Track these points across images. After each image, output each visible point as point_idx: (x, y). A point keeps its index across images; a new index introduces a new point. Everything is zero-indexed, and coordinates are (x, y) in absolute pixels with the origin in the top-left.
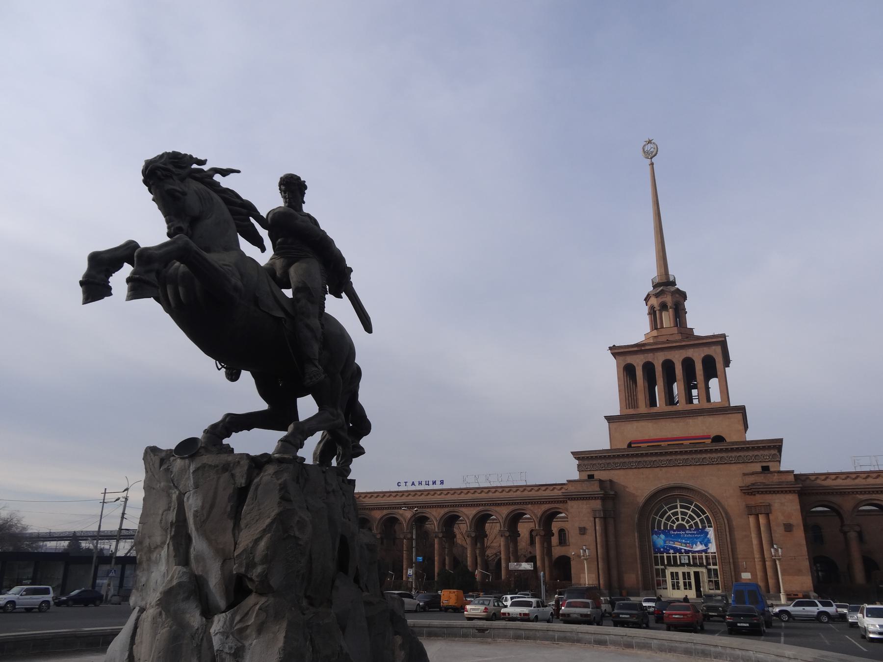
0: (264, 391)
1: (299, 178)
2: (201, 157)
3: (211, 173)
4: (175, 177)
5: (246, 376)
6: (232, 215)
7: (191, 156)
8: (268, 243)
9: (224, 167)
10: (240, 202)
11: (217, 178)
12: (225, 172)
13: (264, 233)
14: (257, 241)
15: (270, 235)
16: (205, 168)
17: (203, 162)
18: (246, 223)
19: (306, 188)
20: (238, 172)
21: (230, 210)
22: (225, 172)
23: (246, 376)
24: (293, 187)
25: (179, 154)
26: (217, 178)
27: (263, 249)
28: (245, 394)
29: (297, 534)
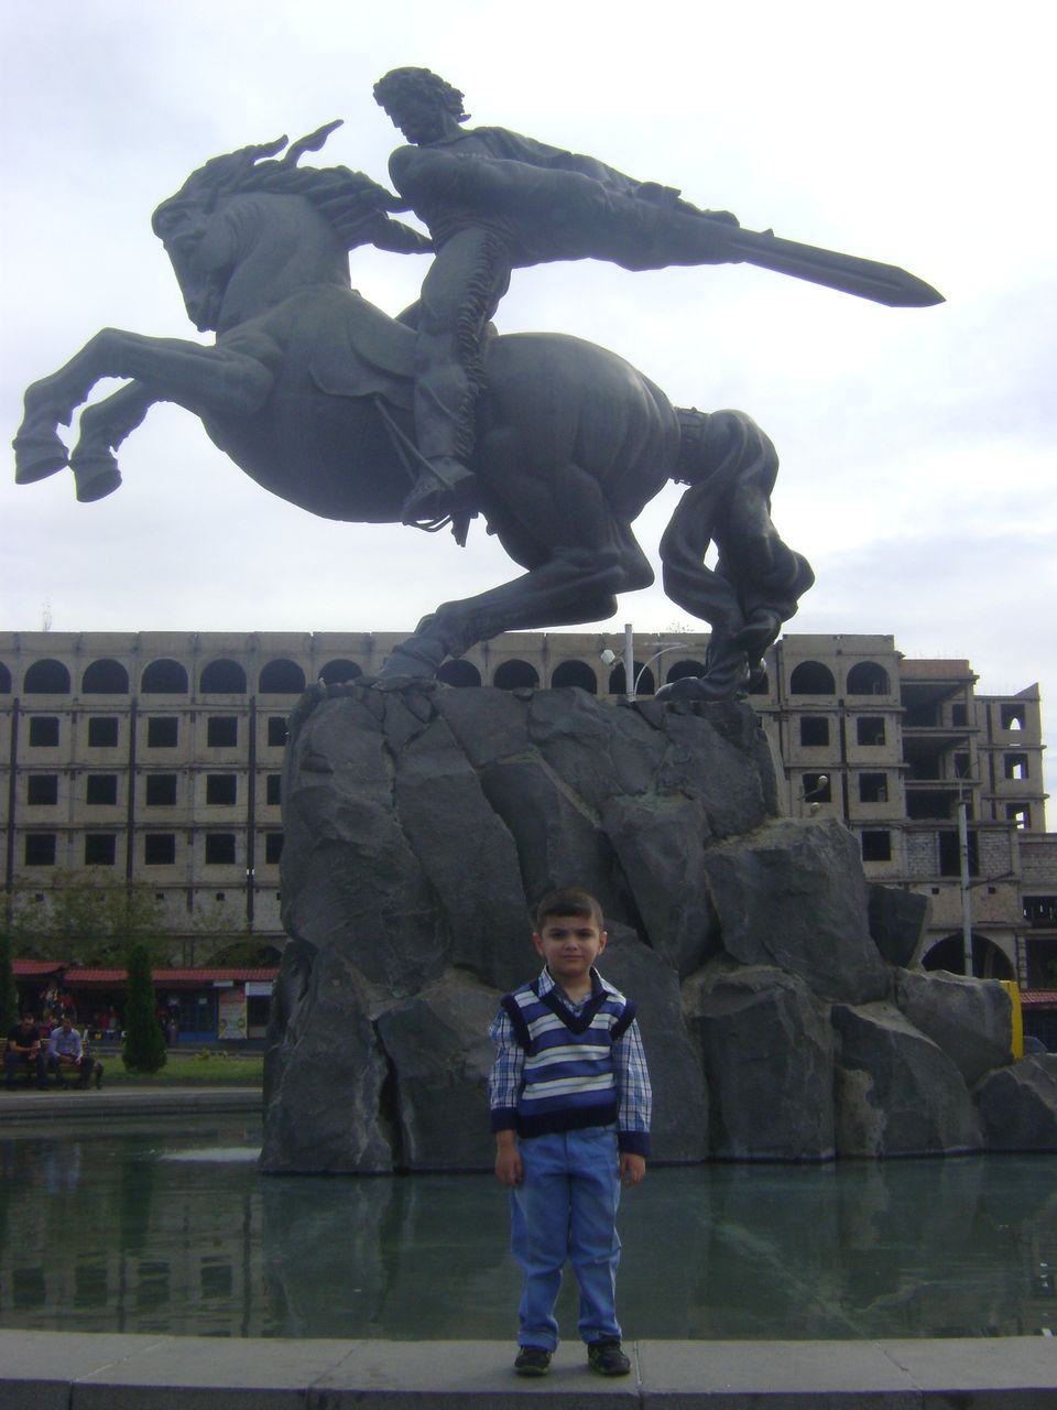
0: (517, 549)
2: (273, 138)
5: (479, 524)
9: (311, 129)
11: (307, 160)
12: (315, 141)
13: (409, 219)
14: (403, 242)
15: (421, 216)
16: (280, 156)
20: (338, 123)
22: (315, 141)
23: (479, 524)
24: (417, 99)
28: (479, 563)
29: (347, 834)
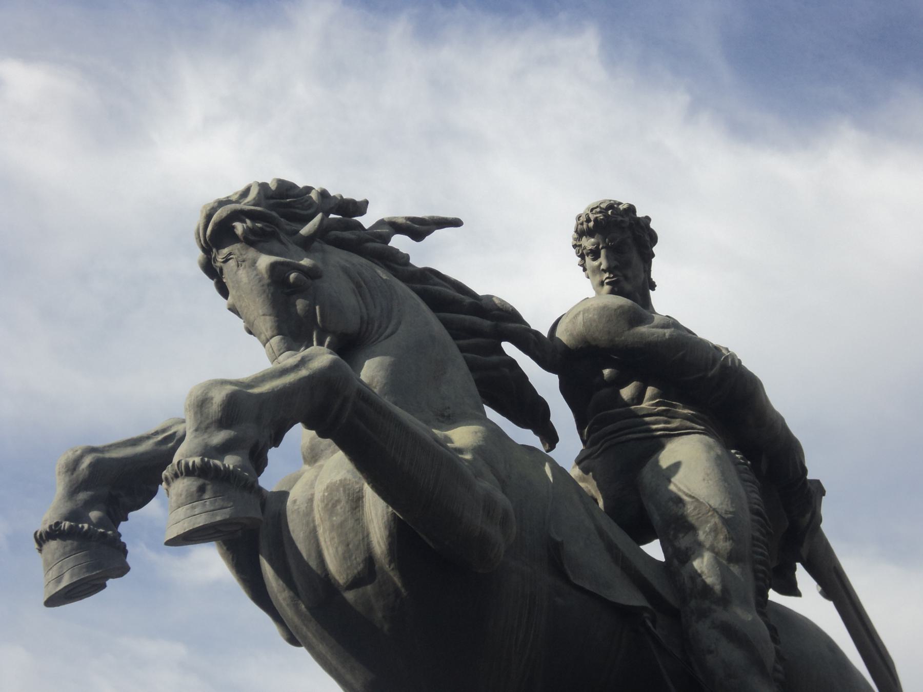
1: (631, 209)
3: (385, 230)
4: (283, 236)
6: (455, 337)
7: (324, 194)
8: (562, 416)
10: (468, 300)
11: (400, 242)
15: (566, 390)
17: (360, 208)
18: (495, 358)
19: (653, 238)
20: (456, 223)
21: (446, 324)
22: (419, 229)
25: (293, 186)
26: (400, 242)
27: (550, 437)
